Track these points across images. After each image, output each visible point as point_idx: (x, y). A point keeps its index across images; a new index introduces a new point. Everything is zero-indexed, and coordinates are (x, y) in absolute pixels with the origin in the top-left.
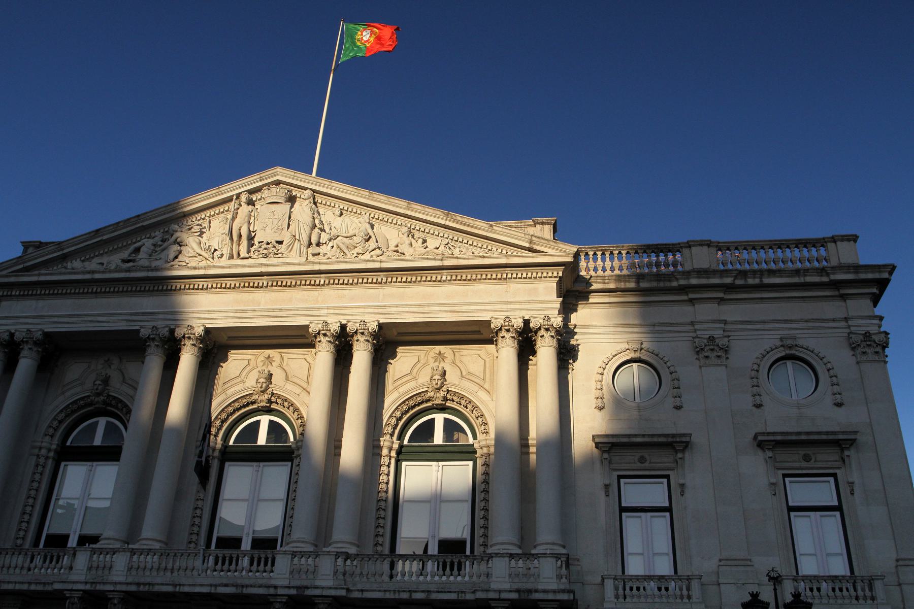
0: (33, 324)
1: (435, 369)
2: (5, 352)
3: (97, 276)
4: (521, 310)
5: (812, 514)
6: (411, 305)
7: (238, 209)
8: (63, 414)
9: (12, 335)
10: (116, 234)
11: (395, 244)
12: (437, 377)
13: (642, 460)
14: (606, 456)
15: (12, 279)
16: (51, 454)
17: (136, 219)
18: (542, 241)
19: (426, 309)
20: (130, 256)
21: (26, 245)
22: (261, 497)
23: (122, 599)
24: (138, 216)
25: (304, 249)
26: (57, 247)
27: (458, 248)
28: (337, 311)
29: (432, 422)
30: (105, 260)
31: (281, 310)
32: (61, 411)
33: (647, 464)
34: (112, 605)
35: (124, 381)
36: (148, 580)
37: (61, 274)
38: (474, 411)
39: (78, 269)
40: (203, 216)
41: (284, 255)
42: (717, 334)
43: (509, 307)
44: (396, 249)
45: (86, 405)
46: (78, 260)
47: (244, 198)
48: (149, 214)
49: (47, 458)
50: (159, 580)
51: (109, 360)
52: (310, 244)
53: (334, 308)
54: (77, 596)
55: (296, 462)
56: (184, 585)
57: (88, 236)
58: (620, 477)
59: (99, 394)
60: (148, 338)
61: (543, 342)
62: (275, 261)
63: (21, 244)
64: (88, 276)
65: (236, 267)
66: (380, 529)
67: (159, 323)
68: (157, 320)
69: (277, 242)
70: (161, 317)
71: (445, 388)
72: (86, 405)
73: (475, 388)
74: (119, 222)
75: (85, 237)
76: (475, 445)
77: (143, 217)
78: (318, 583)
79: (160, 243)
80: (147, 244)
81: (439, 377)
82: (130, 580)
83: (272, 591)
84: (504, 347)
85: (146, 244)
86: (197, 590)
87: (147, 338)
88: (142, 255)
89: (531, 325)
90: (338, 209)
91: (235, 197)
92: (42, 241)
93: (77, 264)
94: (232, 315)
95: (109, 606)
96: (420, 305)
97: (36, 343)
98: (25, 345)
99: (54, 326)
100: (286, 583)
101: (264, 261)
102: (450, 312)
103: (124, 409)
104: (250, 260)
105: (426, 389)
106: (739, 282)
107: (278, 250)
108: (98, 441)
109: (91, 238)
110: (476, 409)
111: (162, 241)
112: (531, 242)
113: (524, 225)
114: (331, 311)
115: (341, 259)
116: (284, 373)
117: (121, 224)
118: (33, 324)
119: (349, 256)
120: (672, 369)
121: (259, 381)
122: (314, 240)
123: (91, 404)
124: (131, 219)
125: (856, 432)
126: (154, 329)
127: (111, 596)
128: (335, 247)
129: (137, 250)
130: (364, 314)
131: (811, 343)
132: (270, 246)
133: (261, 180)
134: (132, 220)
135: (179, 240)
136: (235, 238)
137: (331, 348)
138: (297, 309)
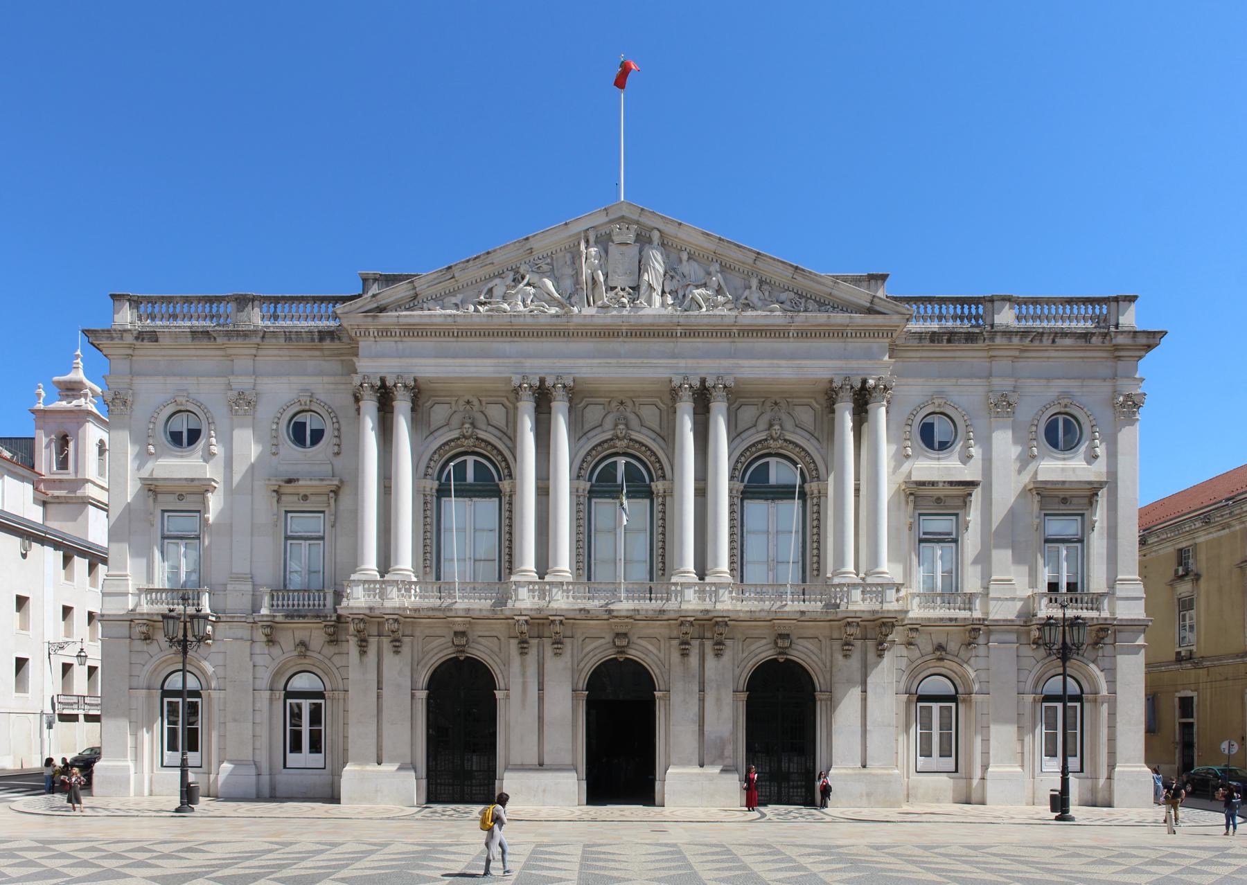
12: (777, 427)
14: (912, 498)
32: (435, 453)
35: (489, 424)
49: (432, 496)
58: (920, 514)
120: (968, 422)
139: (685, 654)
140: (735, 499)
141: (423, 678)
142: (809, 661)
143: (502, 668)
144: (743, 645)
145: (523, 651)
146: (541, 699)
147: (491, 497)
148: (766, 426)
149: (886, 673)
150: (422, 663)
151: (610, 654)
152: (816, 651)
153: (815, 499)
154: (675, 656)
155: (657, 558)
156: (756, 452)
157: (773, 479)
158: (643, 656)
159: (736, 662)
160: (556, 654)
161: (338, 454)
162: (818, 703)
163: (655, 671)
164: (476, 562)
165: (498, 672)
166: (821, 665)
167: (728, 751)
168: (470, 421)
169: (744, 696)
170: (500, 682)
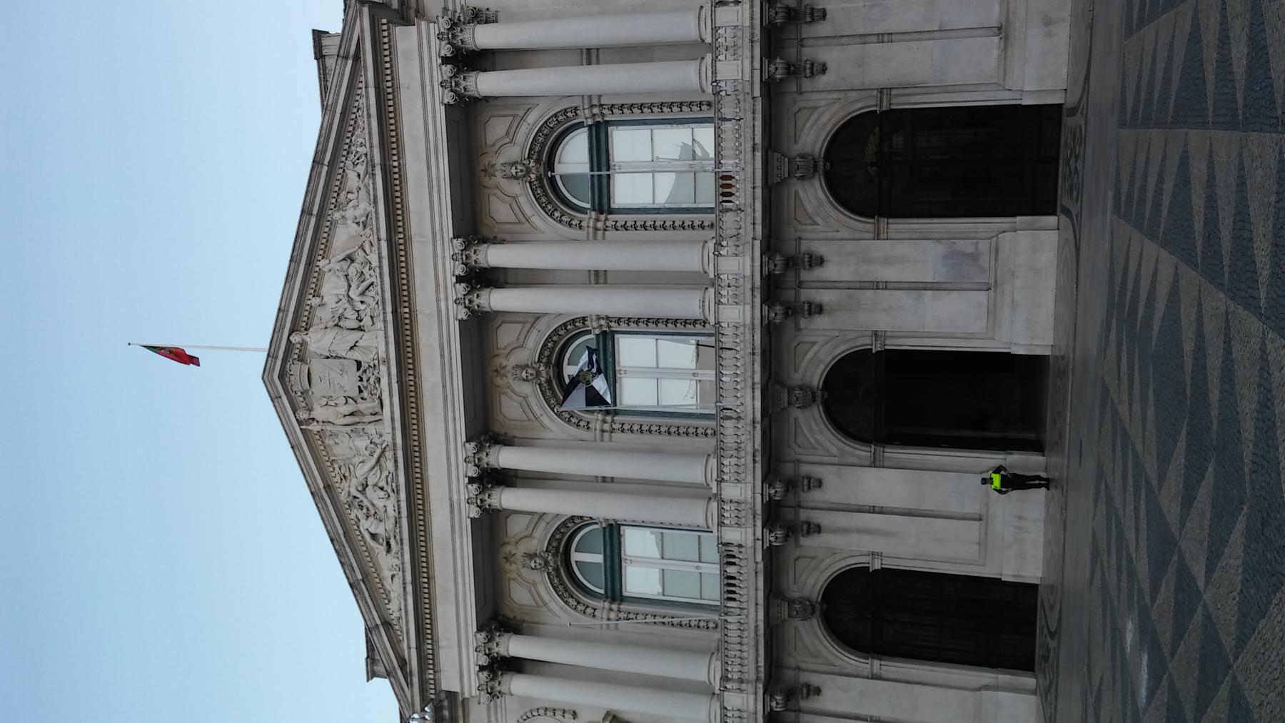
0: (468, 646)
1: (504, 173)
2: (501, 675)
3: (409, 578)
4: (431, 68)
6: (431, 202)
7: (318, 422)
8: (570, 600)
9: (482, 668)
10: (355, 565)
11: (355, 225)
12: (513, 171)
15: (416, 680)
16: (615, 607)
17: (335, 542)
18: (344, 42)
19: (435, 183)
20: (382, 545)
21: (371, 674)
22: (655, 366)
23: (770, 485)
24: (332, 540)
25: (366, 336)
26: (373, 633)
27: (359, 149)
28: (442, 289)
30: (387, 574)
31: (442, 356)
32: (566, 603)
34: (777, 495)
36: (750, 458)
37: (407, 622)
38: (551, 126)
39: (399, 602)
40: (329, 464)
41: (376, 357)
43: (428, 83)
44: (361, 224)
45: (559, 576)
46: (388, 607)
47: (303, 415)
48: (329, 528)
49: (619, 611)
50: (750, 449)
51: (506, 558)
52: (360, 329)
53: (438, 292)
54: (768, 534)
55: (615, 327)
56: (754, 418)
57: (358, 598)
59: (546, 563)
60: (480, 507)
61: (468, 41)
63: (370, 682)
64: (409, 589)
65: (392, 413)
66: (686, 224)
67: (462, 498)
68: (459, 499)
69: (358, 370)
70: (455, 497)
71: (526, 162)
72: (559, 576)
73: (524, 128)
74: (341, 562)
75: (360, 601)
76: (590, 122)
77: (332, 534)
78: (748, 273)
79: (365, 511)
80: (364, 524)
81: (514, 168)
82: (750, 478)
84: (477, 88)
85: (366, 528)
86: (758, 404)
87: (480, 508)
88: (380, 530)
89: (449, 55)
90: (314, 299)
91: (303, 427)
92: (365, 656)
93: (393, 606)
94: (450, 414)
95: (778, 498)
97: (490, 640)
98: (493, 651)
99: (469, 622)
100: (748, 307)
101: (384, 381)
102: (437, 154)
103: (562, 530)
104: (383, 397)
105: (528, 184)
107: (369, 366)
108: (598, 558)
109: (361, 592)
110: (548, 124)
111: (362, 509)
112: (346, 58)
113: (323, 71)
114: (442, 296)
115: (379, 288)
116: (517, 350)
117: (343, 560)
118: (468, 646)
119: (373, 279)
121: (525, 377)
122: (354, 324)
123: (557, 570)
124: (335, 549)
126: (470, 501)
127: (768, 497)
128: (363, 299)
129: (374, 536)
130: (444, 257)
132: (365, 379)
133: (280, 397)
134: (337, 547)
135: (360, 488)
136: (357, 419)
137: (485, 293)
138: (441, 336)
139: (818, 309)
140: (609, 224)
141: (852, 662)
142: (828, 128)
143: (837, 557)
144: (804, 224)
145: (819, 529)
146: (882, 511)
147: (620, 536)
148: (515, 182)
149: (849, 5)
150: (831, 658)
151: (817, 412)
152: (815, 116)
153: (604, 111)
154: (820, 322)
155: (688, 329)
156: (546, 195)
157: (585, 169)
158: (822, 367)
159: (830, 234)
160: (820, 483)
161: (575, 714)
162: (893, 107)
163: (842, 349)
164: (702, 560)
165: (843, 564)
166: (836, 107)
167: (966, 246)
168: (528, 561)
169: (883, 221)
170: (861, 561)
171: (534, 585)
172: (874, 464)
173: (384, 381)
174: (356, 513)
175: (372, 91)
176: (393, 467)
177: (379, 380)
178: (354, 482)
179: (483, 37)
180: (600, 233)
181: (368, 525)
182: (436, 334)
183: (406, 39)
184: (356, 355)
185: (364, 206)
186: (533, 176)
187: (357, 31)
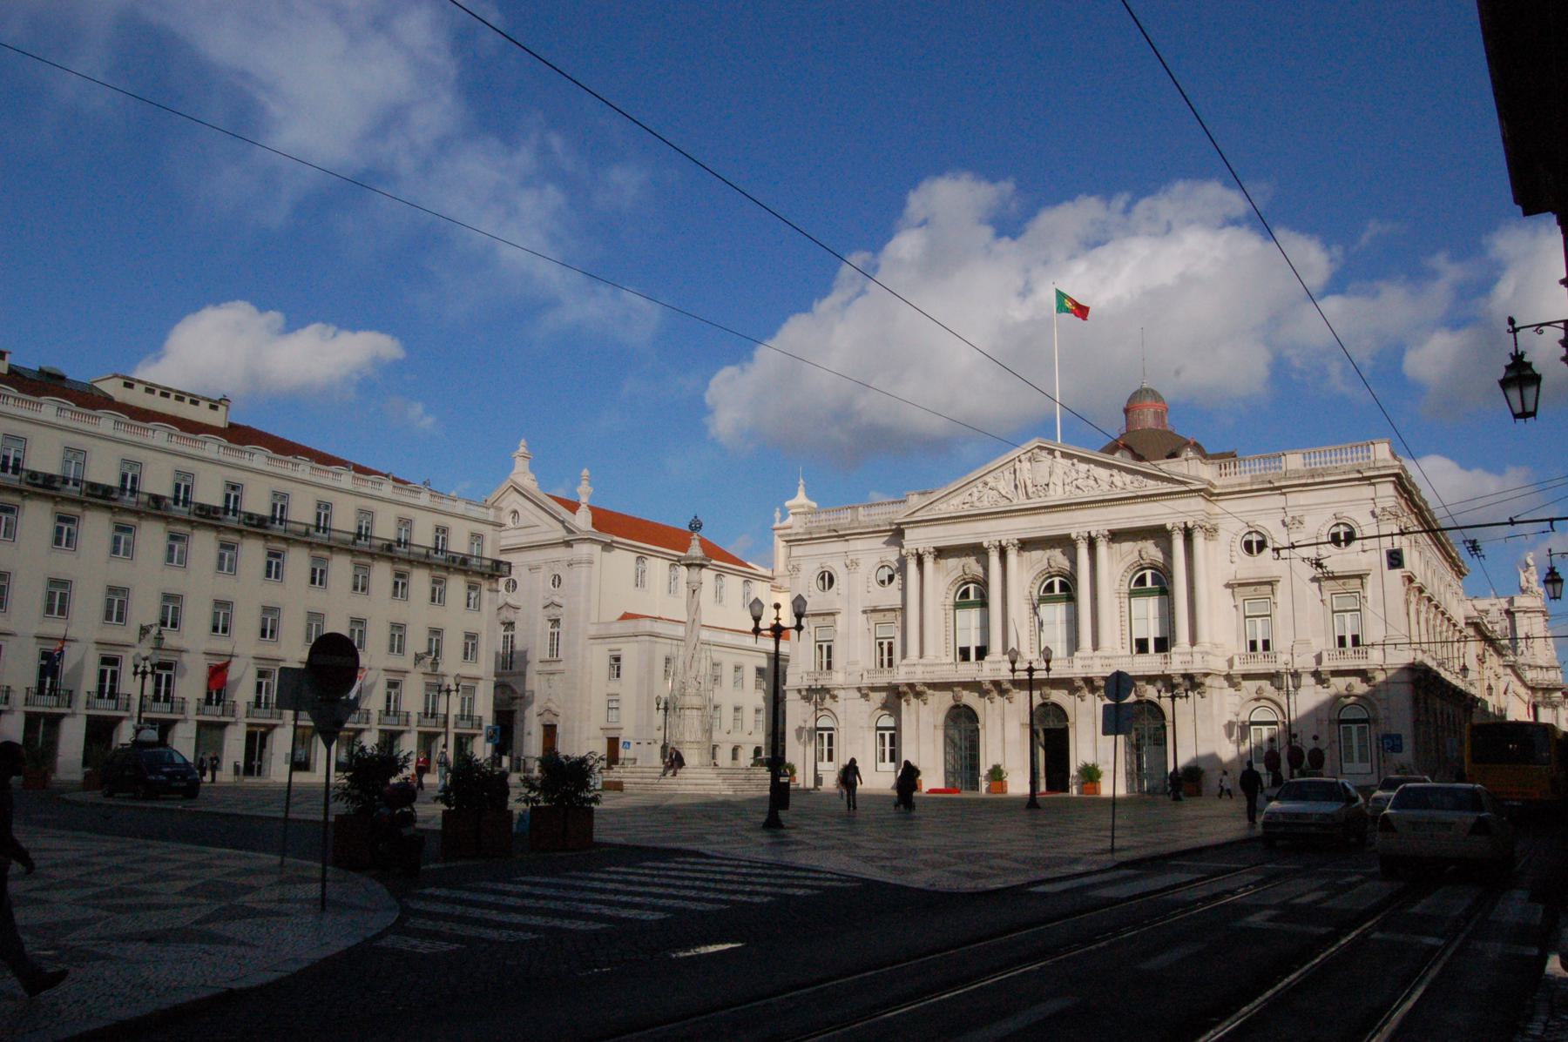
5: (1344, 614)
13: (1255, 590)
19: (1131, 520)
29: (1144, 575)
33: (1258, 592)
42: (1296, 514)
47: (1023, 458)
52: (1064, 485)
58: (1244, 600)
62: (1046, 499)
83: (1073, 676)
96: (1128, 518)
101: (1040, 500)
106: (1310, 481)
125: (1371, 570)
131: (1353, 515)
171: (957, 568)
172: (1022, 724)
173: (1040, 500)
174: (980, 485)
175: (1169, 490)
176: (1003, 505)
177: (1040, 497)
178: (994, 484)
179: (1199, 540)
180: (1117, 595)
181: (976, 495)
182: (1063, 522)
183: (1197, 504)
184: (1051, 486)
185: (1120, 484)
186: (1142, 562)
187: (1197, 483)
